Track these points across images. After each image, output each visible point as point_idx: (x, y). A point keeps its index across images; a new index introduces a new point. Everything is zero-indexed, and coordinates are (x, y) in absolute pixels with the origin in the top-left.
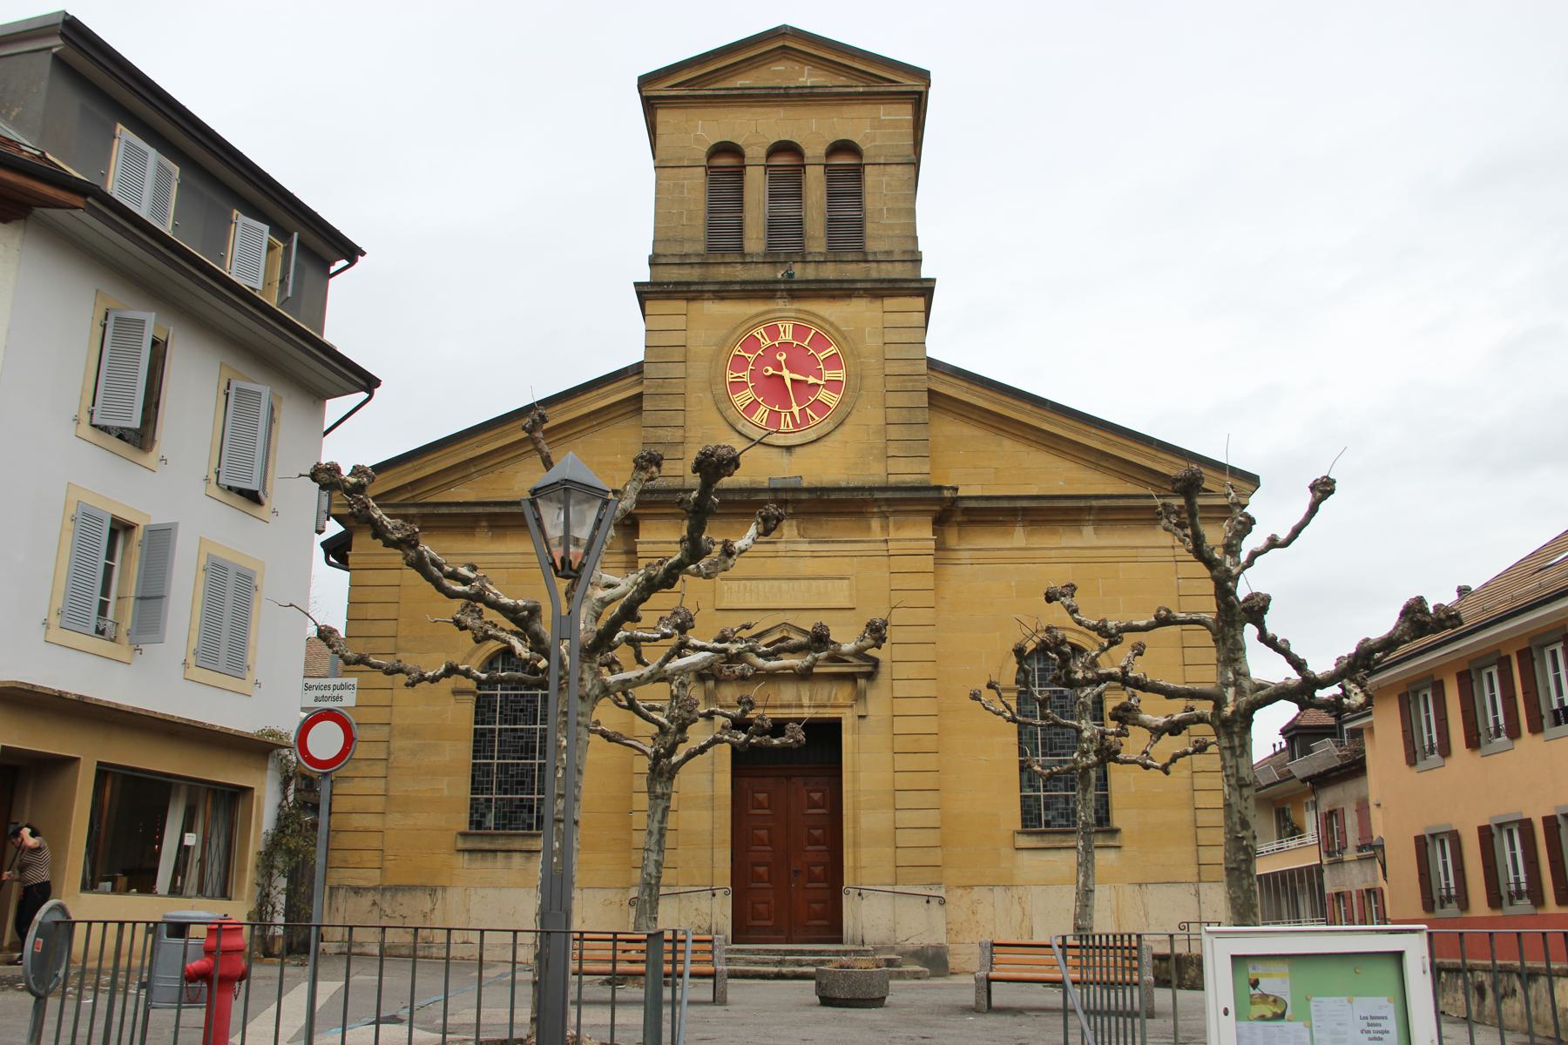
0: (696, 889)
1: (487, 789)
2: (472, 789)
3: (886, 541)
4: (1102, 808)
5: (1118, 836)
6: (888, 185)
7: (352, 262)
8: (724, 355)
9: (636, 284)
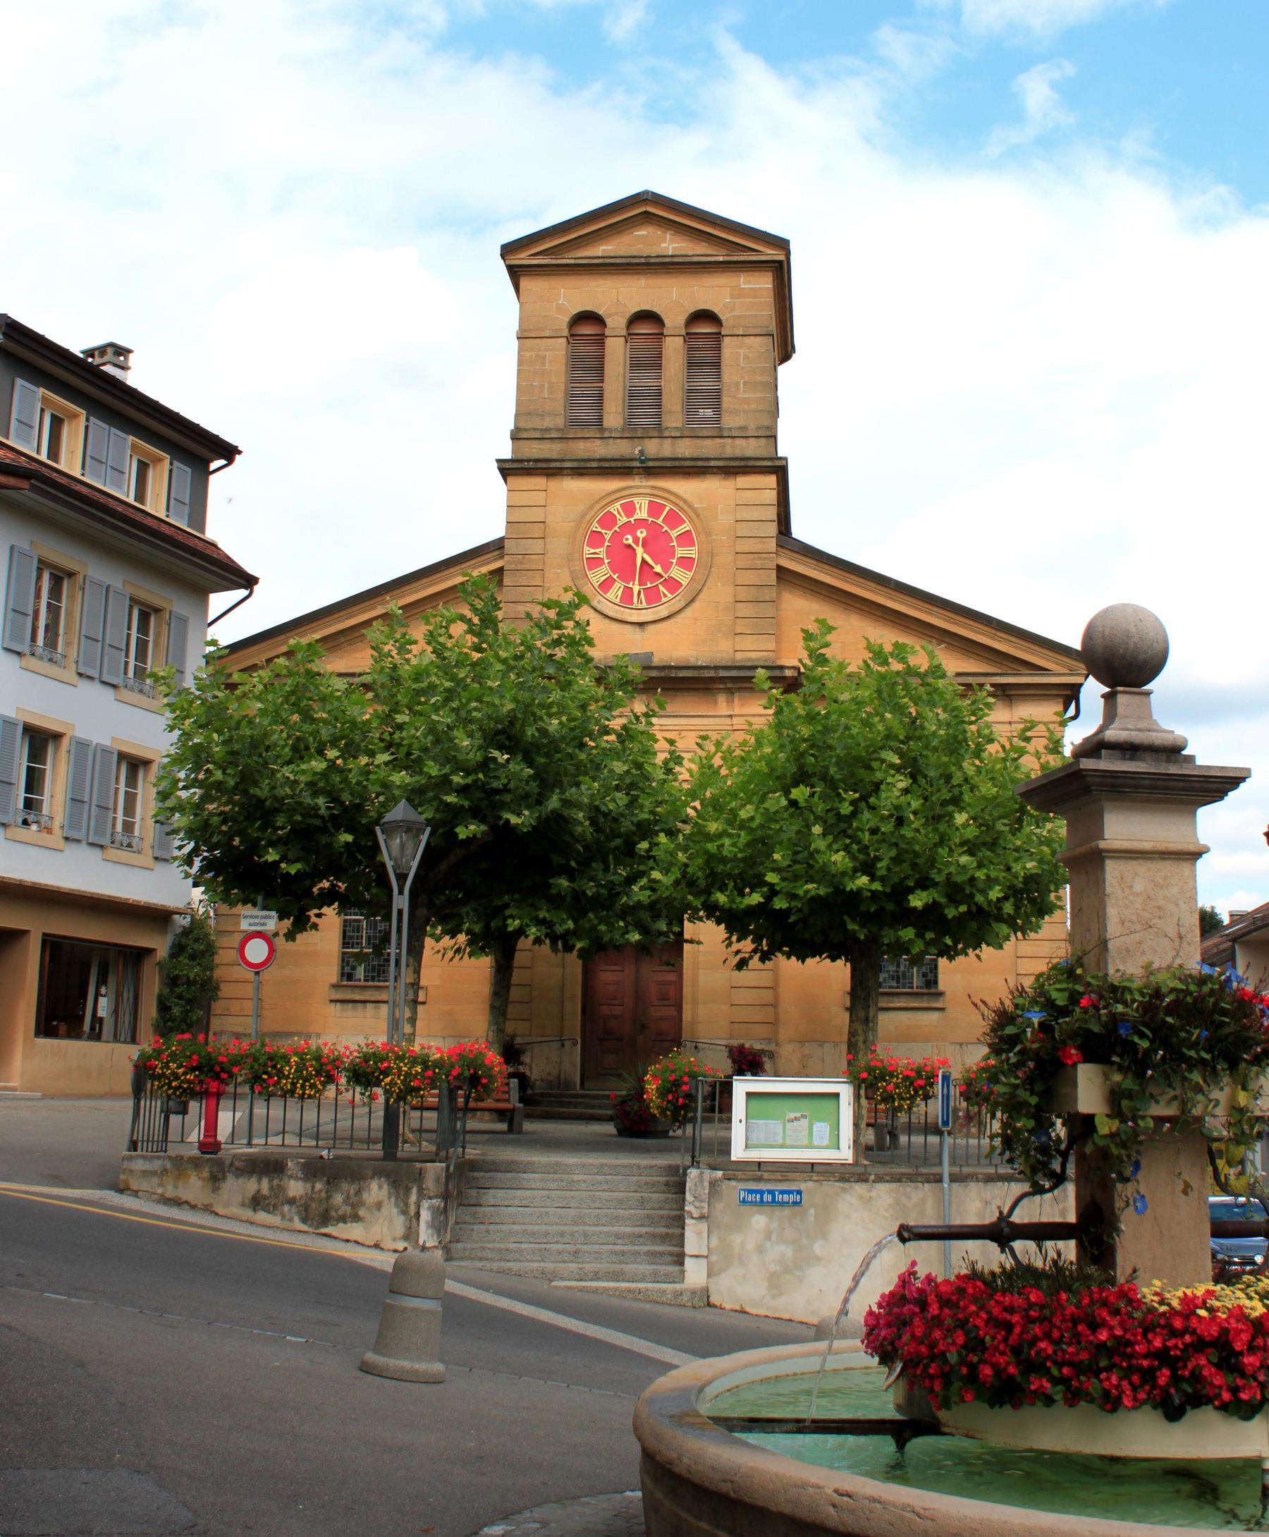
0: (546, 1039)
1: (358, 943)
2: (344, 943)
3: (731, 716)
4: (931, 972)
5: (941, 999)
6: (746, 357)
7: (230, 461)
8: (581, 531)
9: (498, 461)
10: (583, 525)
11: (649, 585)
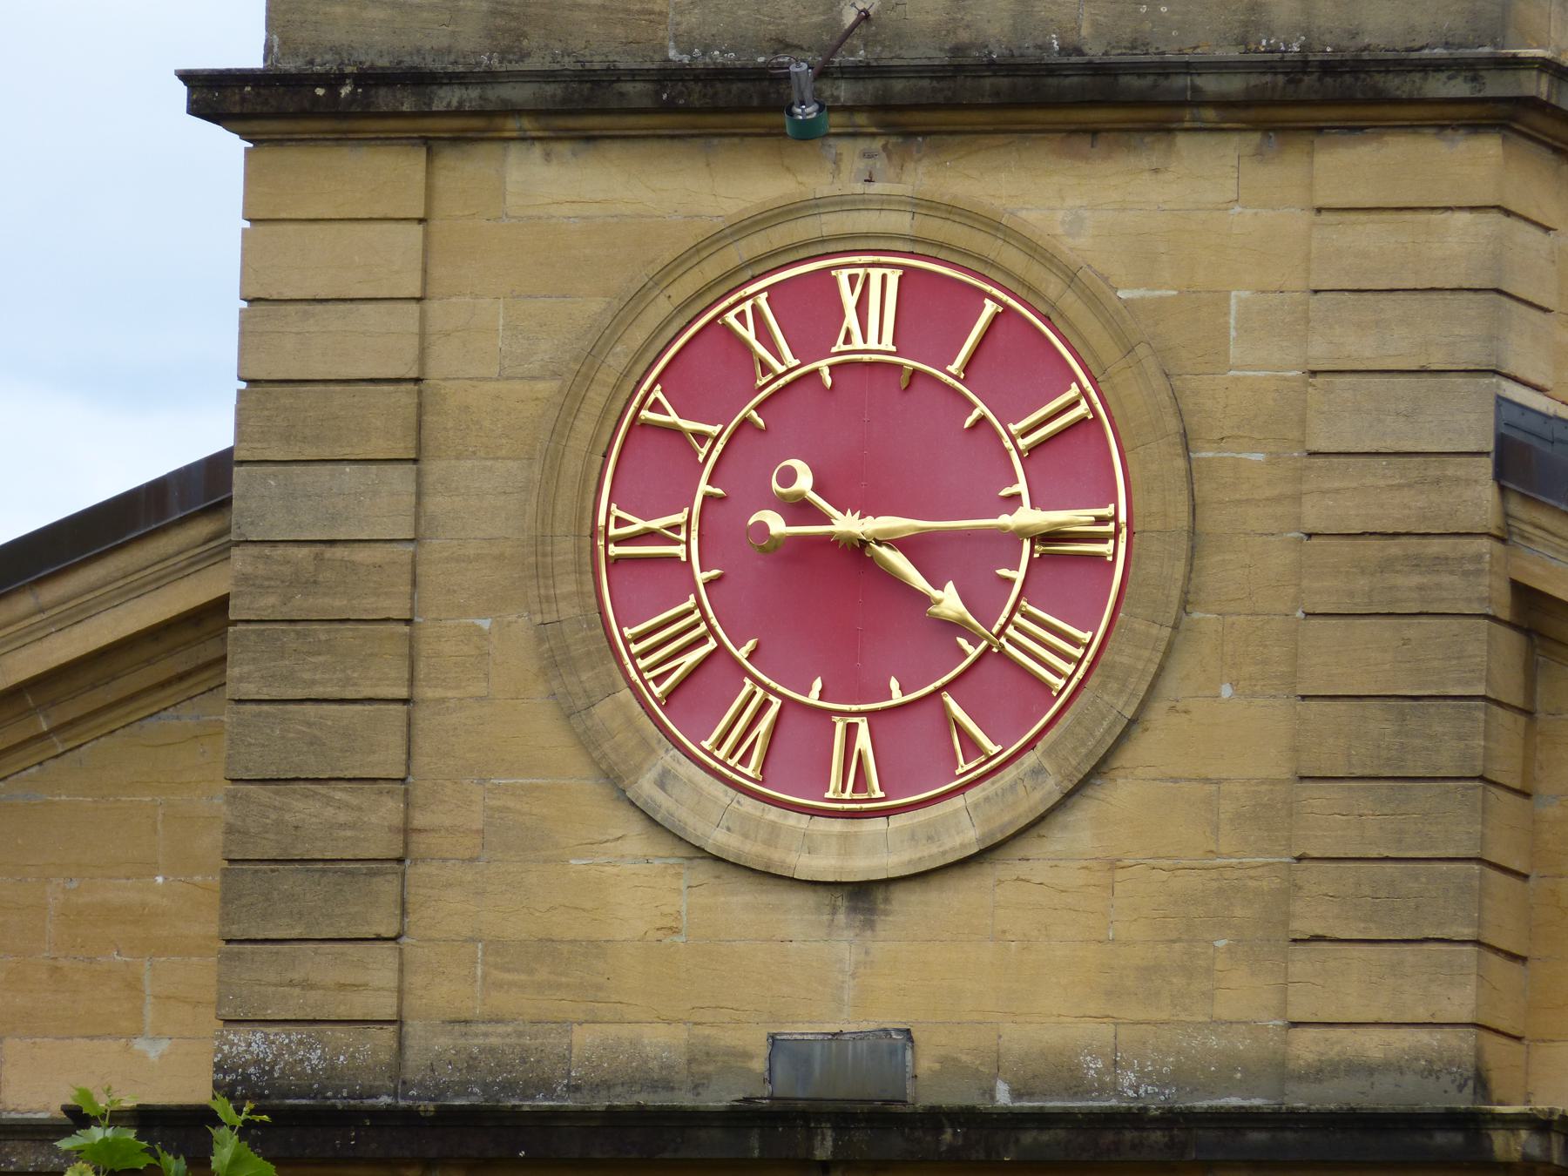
8: (585, 426)
10: (597, 397)
11: (898, 698)
